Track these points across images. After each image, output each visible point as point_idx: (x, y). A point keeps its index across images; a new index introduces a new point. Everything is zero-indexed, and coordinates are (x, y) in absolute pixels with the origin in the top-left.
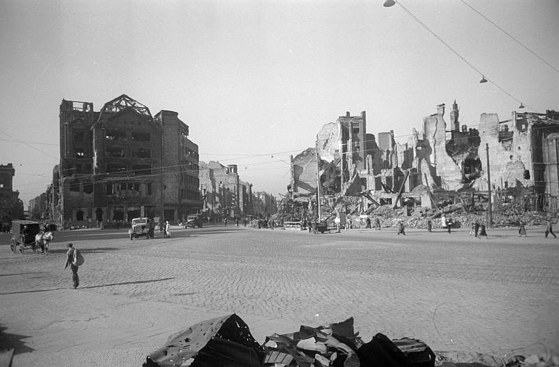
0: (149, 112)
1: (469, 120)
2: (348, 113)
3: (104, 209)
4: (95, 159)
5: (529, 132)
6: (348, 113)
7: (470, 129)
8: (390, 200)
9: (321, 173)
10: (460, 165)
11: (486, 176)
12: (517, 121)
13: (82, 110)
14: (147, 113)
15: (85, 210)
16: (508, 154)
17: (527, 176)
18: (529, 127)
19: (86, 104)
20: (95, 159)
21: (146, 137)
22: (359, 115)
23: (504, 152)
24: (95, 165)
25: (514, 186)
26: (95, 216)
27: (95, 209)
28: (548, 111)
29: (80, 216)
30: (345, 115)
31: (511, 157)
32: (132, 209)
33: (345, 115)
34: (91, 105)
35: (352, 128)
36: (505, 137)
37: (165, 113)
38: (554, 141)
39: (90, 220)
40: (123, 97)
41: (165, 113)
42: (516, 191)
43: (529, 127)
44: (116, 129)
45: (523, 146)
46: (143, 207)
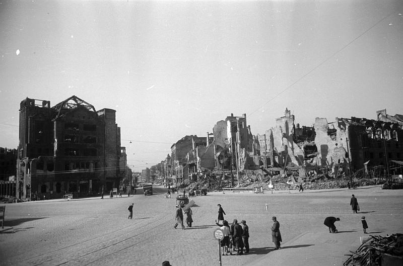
0: (94, 109)
1: (304, 121)
2: (232, 114)
3: (62, 183)
4: (56, 145)
5: (347, 130)
6: (232, 114)
7: (303, 126)
8: (279, 172)
9: (219, 154)
10: (303, 149)
11: (320, 156)
12: (339, 123)
13: (41, 107)
14: (92, 110)
15: (47, 184)
16: (334, 142)
17: (347, 155)
18: (347, 127)
19: (45, 102)
20: (56, 145)
21: (93, 128)
22: (241, 116)
23: (332, 141)
24: (56, 149)
25: (343, 162)
26: (55, 190)
27: (56, 183)
28: (352, 117)
29: (44, 190)
30: (230, 116)
31: (337, 144)
32: (83, 182)
33: (230, 116)
34: (49, 103)
35: (239, 125)
36: (331, 133)
37: (108, 111)
38: (360, 135)
39: (52, 192)
40: (74, 98)
41: (107, 110)
42: (343, 166)
43: (347, 127)
44: (72, 122)
45: (343, 137)
46: (91, 181)
